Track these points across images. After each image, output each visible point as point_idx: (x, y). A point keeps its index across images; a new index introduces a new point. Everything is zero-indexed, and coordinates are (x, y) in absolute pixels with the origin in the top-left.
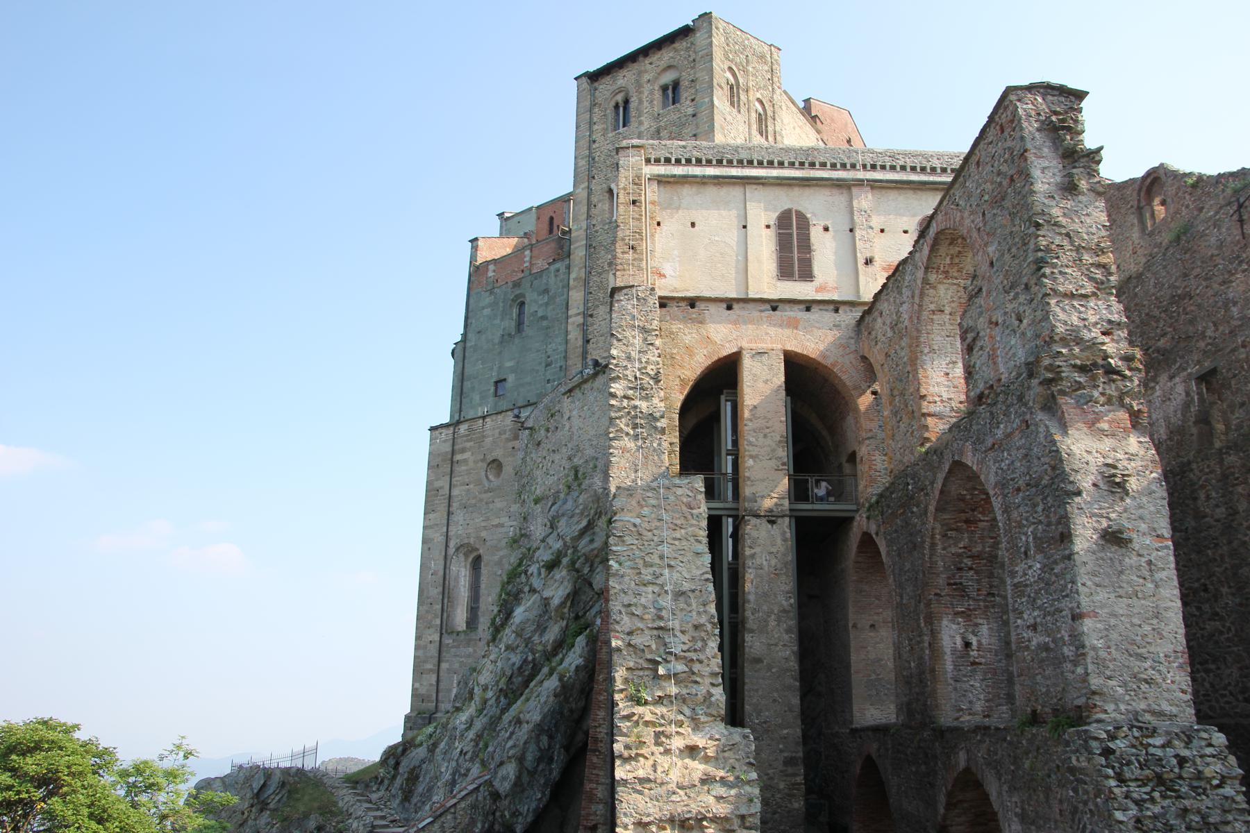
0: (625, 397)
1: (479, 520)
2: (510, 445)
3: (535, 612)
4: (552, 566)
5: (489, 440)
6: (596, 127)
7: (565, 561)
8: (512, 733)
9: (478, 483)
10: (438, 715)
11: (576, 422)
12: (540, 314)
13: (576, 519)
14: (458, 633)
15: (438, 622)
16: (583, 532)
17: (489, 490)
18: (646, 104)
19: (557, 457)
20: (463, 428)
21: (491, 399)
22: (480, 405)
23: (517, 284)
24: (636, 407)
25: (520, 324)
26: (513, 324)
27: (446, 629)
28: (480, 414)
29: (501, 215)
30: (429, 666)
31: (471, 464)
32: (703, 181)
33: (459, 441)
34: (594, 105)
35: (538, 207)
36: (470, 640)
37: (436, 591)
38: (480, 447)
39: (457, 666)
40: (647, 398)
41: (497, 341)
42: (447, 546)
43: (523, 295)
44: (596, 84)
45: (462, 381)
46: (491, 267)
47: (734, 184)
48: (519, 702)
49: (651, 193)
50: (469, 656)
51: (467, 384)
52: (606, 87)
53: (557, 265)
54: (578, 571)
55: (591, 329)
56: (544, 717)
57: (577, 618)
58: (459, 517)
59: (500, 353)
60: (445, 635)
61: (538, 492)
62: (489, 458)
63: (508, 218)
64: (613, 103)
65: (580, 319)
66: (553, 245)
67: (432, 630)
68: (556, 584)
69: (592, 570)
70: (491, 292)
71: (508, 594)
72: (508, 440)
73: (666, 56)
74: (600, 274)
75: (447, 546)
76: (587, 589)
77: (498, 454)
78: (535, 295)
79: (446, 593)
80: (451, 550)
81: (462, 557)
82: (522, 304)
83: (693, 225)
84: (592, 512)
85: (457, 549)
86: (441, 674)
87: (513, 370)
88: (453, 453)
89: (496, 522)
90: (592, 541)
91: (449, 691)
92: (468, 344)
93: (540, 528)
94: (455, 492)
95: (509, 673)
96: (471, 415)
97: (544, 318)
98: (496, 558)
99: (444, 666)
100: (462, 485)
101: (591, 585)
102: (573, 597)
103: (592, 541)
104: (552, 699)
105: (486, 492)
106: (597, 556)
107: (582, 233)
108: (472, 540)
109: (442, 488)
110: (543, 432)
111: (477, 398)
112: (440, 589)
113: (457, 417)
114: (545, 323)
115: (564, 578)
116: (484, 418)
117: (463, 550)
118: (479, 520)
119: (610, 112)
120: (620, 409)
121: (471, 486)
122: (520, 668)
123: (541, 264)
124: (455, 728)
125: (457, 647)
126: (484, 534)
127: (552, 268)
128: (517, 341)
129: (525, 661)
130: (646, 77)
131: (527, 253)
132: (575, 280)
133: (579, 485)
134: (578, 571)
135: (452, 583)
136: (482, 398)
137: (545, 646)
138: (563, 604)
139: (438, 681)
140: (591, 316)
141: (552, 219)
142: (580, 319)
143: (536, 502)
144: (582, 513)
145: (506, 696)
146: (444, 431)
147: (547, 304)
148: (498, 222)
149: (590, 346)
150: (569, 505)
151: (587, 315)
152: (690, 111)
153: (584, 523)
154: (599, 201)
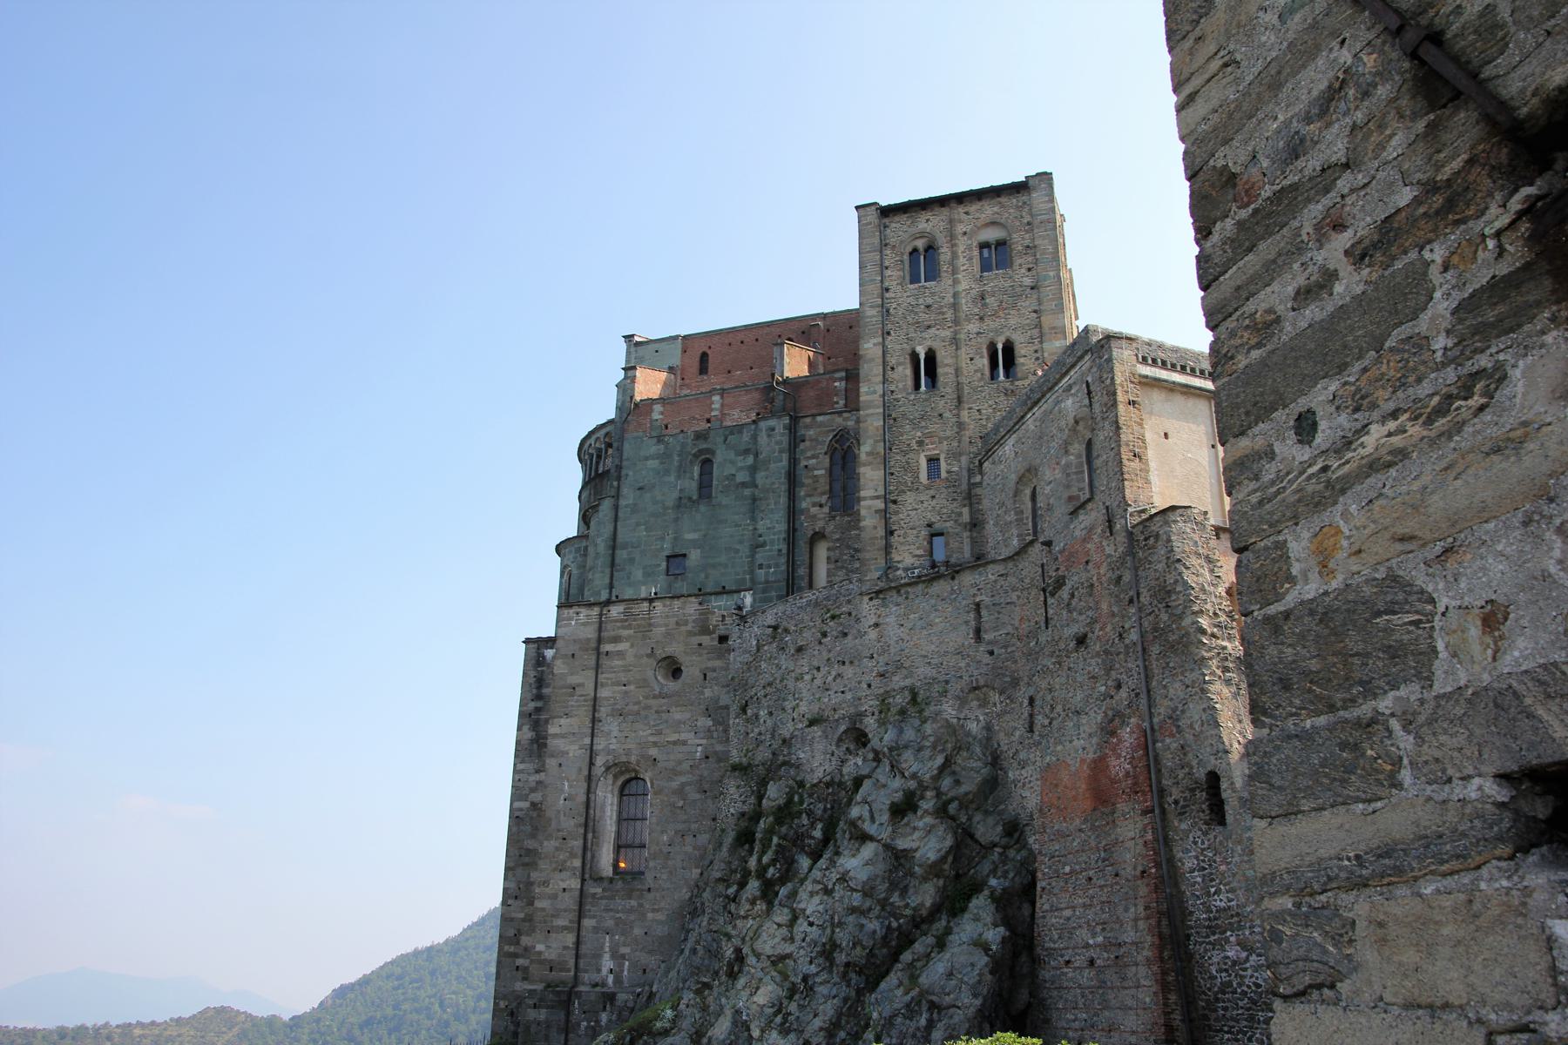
0: (1213, 635)
1: (645, 733)
2: (696, 640)
3: (880, 868)
4: (903, 809)
5: (659, 631)
6: (888, 273)
7: (927, 804)
8: (931, 1025)
9: (643, 684)
10: (581, 988)
11: (893, 631)
12: (742, 477)
13: (927, 753)
14: (611, 880)
15: (577, 863)
16: (943, 769)
17: (661, 696)
18: (962, 260)
19: (848, 671)
20: (616, 611)
21: (662, 577)
22: (644, 584)
23: (700, 436)
24: (1224, 648)
25: (705, 486)
26: (694, 485)
27: (588, 873)
28: (643, 595)
29: (629, 338)
30: (560, 922)
31: (630, 658)
32: (1172, 388)
33: (609, 626)
34: (884, 245)
35: (685, 337)
36: (632, 890)
37: (572, 822)
38: (644, 638)
39: (610, 923)
40: (1230, 638)
41: (670, 503)
42: (591, 764)
43: (713, 453)
44: (886, 221)
45: (614, 548)
46: (658, 408)
47: (1199, 396)
48: (892, 979)
49: (1134, 392)
50: (631, 911)
51: (621, 555)
52: (899, 228)
53: (772, 423)
54: (953, 818)
55: (894, 518)
56: (985, 1000)
57: (958, 876)
58: (611, 726)
59: (676, 520)
60: (589, 882)
61: (803, 708)
62: (660, 653)
63: (638, 344)
64: (909, 249)
65: (880, 504)
66: (756, 395)
67: (565, 874)
68: (917, 835)
69: (970, 819)
70: (660, 439)
71: (783, 838)
72: (690, 634)
73: (988, 210)
74: (906, 453)
75: (591, 764)
76: (969, 841)
77: (675, 649)
78: (732, 455)
79: (589, 825)
80: (599, 769)
81: (610, 777)
82: (707, 464)
83: (1166, 435)
84: (949, 745)
85: (608, 769)
86: (583, 933)
87: (695, 544)
88: (600, 641)
89: (674, 737)
90: (957, 782)
91: (598, 956)
92: (622, 502)
93: (819, 757)
94: (604, 693)
95: (868, 943)
96: (629, 593)
97: (744, 485)
98: (675, 785)
99: (588, 923)
100: (618, 684)
101: (972, 836)
102: (956, 850)
103: (957, 782)
104: (989, 977)
105: (655, 697)
106: (972, 802)
107: (877, 398)
108: (633, 759)
109: (582, 685)
110: (808, 636)
111: (638, 574)
112: (582, 820)
113: (604, 596)
114: (747, 492)
115: (933, 826)
116: (651, 601)
117: (614, 770)
118: (645, 733)
119: (906, 257)
120: (1211, 649)
121: (632, 687)
122: (884, 938)
123: (737, 416)
124: (738, 1012)
125: (612, 898)
126: (653, 752)
127: (763, 425)
128: (703, 508)
129: (889, 927)
130: (960, 228)
131: (716, 398)
132: (868, 454)
133: (921, 711)
134: (953, 818)
135: (598, 813)
136: (647, 575)
137: (914, 909)
138: (943, 859)
139: (578, 943)
140: (895, 502)
141: (704, 356)
142: (880, 504)
143: (812, 723)
144: (934, 747)
145: (859, 973)
146: (584, 612)
147: (753, 469)
148: (623, 346)
149: (894, 540)
150: (909, 734)
151: (890, 500)
152: (1027, 281)
153: (940, 760)
154: (899, 364)
